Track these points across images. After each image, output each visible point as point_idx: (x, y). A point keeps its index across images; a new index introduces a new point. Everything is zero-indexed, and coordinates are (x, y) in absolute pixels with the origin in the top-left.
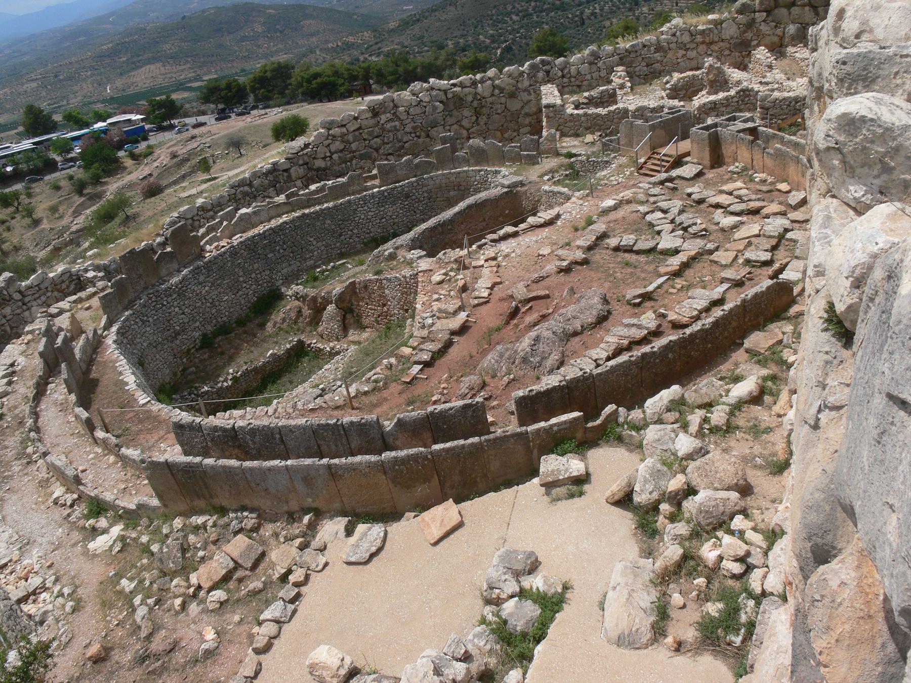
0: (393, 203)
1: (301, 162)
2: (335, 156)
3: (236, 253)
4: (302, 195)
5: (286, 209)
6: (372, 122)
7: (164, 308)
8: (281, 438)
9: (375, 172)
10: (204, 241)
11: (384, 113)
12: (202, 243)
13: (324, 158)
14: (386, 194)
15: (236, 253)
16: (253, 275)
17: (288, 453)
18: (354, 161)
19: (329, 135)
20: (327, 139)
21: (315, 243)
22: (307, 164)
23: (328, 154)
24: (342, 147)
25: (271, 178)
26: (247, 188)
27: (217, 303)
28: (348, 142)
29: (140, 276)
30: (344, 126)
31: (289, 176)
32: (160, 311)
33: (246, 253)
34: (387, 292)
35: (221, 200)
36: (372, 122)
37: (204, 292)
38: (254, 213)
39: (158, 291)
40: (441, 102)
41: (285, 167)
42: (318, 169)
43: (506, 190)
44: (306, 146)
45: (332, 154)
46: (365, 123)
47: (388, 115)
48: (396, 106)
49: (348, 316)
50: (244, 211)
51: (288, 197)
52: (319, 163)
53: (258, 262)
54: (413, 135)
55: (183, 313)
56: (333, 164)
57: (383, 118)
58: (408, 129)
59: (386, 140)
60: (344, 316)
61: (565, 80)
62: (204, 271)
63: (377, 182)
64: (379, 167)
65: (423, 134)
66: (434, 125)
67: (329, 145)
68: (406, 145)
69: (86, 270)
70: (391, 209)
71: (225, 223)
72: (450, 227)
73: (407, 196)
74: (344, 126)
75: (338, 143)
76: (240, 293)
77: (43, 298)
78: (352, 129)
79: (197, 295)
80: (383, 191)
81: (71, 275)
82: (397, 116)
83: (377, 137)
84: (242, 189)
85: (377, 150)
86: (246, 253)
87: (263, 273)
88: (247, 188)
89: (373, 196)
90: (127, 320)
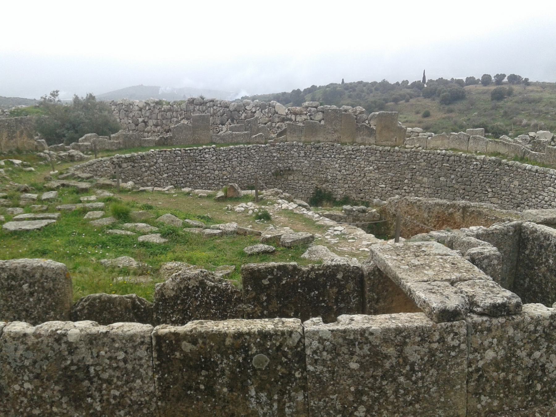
3: (416, 159)
15: (416, 159)
16: (418, 186)
21: (490, 195)
29: (336, 131)
32: (326, 159)
33: (424, 164)
37: (367, 168)
39: (333, 145)
53: (429, 178)
62: (378, 155)
76: (399, 191)
79: (360, 167)
86: (424, 164)
87: (427, 190)
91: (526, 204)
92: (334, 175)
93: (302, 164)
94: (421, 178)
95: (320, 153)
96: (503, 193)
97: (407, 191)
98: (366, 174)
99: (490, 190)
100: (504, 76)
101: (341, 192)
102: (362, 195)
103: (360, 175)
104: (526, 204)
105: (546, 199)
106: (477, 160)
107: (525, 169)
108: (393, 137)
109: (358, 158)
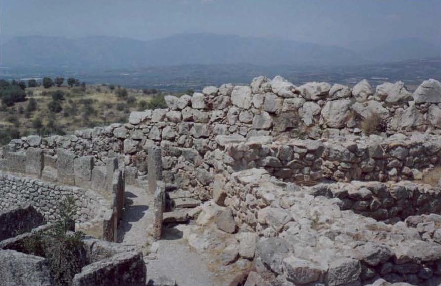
1: (134, 136)
2: (163, 142)
13: (155, 140)
19: (164, 116)
22: (140, 140)
23: (158, 138)
24: (171, 135)
25: (107, 139)
26: (85, 141)
31: (122, 147)
36: (203, 115)
41: (121, 135)
44: (146, 119)
46: (196, 113)
48: (230, 103)
57: (215, 114)
59: (209, 146)
75: (168, 128)
78: (185, 117)
83: (205, 137)
88: (85, 141)
100: (63, 79)
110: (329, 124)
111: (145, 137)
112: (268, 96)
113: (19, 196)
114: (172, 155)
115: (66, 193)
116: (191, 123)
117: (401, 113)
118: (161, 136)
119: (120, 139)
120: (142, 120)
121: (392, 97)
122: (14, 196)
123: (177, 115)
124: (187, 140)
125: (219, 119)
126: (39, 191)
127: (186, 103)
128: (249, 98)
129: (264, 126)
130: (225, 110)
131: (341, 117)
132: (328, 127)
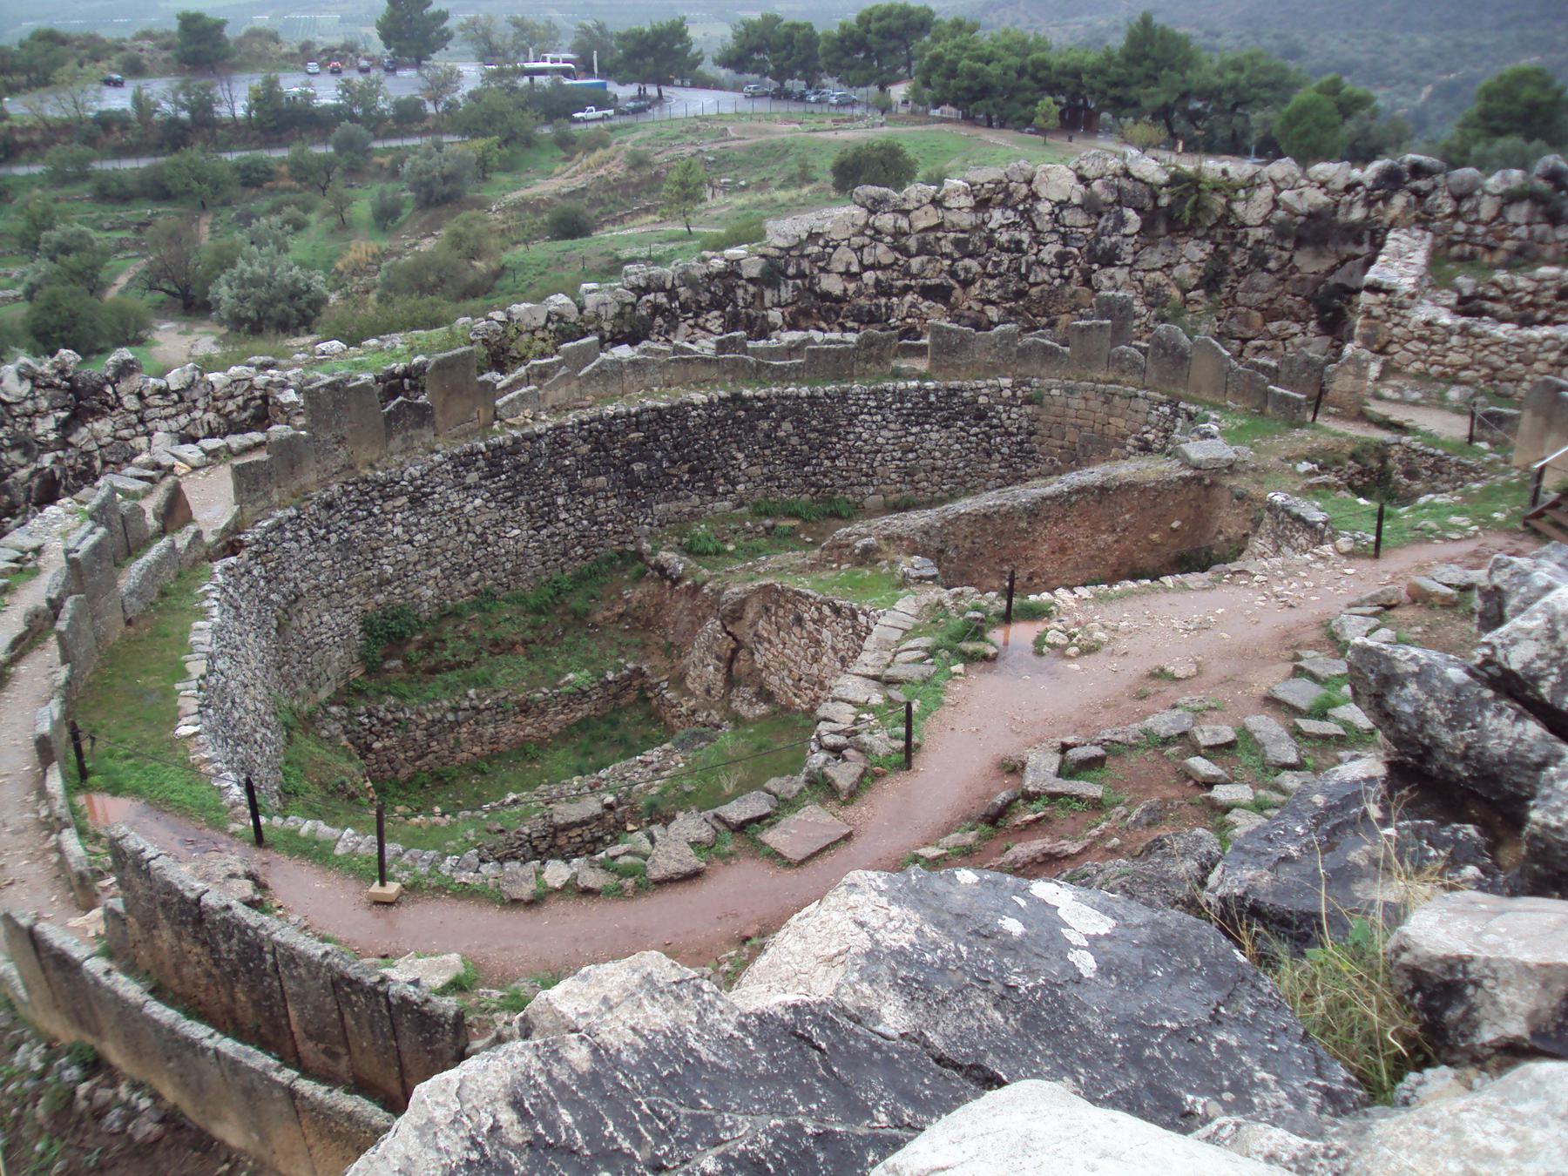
0: (946, 424)
4: (754, 352)
5: (713, 372)
6: (967, 219)
7: (371, 520)
8: (275, 965)
9: (925, 341)
10: (505, 399)
11: (1003, 205)
12: (499, 403)
14: (932, 398)
15: (565, 444)
16: (589, 501)
17: (284, 1000)
18: (909, 298)
19: (867, 225)
20: (861, 233)
23: (855, 268)
26: (662, 298)
27: (491, 538)
28: (904, 251)
29: (341, 441)
30: (906, 213)
32: (362, 526)
34: (826, 633)
35: (602, 310)
38: (634, 363)
40: (1138, 211)
41: (754, 272)
42: (826, 296)
43: (1188, 473)
45: (865, 268)
46: (953, 217)
47: (1010, 213)
48: (1035, 196)
49: (743, 654)
50: (624, 352)
51: (722, 346)
52: (832, 284)
54: (1054, 271)
55: (410, 542)
56: (859, 293)
57: (997, 217)
58: (1049, 252)
60: (735, 652)
61: (1460, 227)
62: (481, 463)
63: (922, 365)
64: (938, 331)
65: (1077, 274)
66: (1109, 258)
67: (861, 248)
68: (1034, 291)
69: (283, 386)
70: (934, 436)
71: (563, 371)
72: (1023, 525)
73: (980, 416)
74: (906, 213)
76: (551, 529)
77: (183, 420)
78: (921, 225)
80: (928, 392)
81: (252, 388)
82: (1030, 220)
83: (971, 256)
84: (651, 297)
85: (966, 284)
88: (662, 298)
89: (901, 396)
90: (279, 527)
91: (822, 456)
92: (400, 557)
93: (314, 567)
94: (589, 480)
95: (338, 516)
96: (767, 452)
97: (571, 520)
98: (472, 521)
99: (740, 456)
101: (429, 593)
102: (475, 575)
103: (459, 530)
104: (822, 456)
105: (865, 436)
106: (695, 407)
107: (798, 397)
108: (473, 409)
109: (439, 489)
110: (1249, 222)
111: (816, 271)
112: (1126, 184)
113: (892, 417)
114: (889, 295)
115: (985, 391)
116: (940, 234)
117: (1351, 204)
118: (861, 262)
119: (751, 280)
120: (804, 236)
121: (1340, 184)
122: (879, 418)
123: (903, 223)
124: (930, 266)
125: (1008, 226)
126: (932, 398)
127: (925, 201)
128: (1081, 187)
129: (1128, 231)
130: (1021, 207)
131: (1264, 211)
132: (1244, 226)
